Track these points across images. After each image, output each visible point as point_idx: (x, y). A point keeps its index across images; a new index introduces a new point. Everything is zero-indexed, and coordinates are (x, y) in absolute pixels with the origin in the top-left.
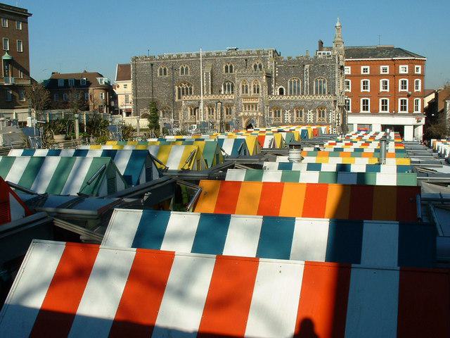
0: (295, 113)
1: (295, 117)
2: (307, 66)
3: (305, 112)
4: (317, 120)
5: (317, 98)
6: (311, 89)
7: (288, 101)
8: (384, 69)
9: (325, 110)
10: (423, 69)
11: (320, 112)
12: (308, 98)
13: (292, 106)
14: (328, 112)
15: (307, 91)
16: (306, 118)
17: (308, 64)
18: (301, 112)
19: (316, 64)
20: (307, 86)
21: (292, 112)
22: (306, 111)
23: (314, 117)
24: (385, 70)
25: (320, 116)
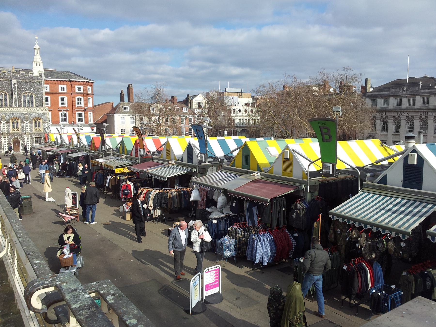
0: (11, 123)
1: (11, 127)
2: (14, 81)
3: (21, 122)
4: (34, 130)
5: (33, 111)
6: (20, 102)
7: (4, 113)
8: (62, 88)
9: (41, 121)
10: (92, 89)
11: (35, 123)
12: (22, 109)
13: (8, 116)
14: (44, 123)
15: (15, 104)
16: (22, 128)
17: (15, 79)
18: (17, 123)
19: (23, 80)
20: (16, 99)
21: (8, 122)
22: (22, 122)
23: (31, 127)
24: (63, 89)
25: (36, 126)
